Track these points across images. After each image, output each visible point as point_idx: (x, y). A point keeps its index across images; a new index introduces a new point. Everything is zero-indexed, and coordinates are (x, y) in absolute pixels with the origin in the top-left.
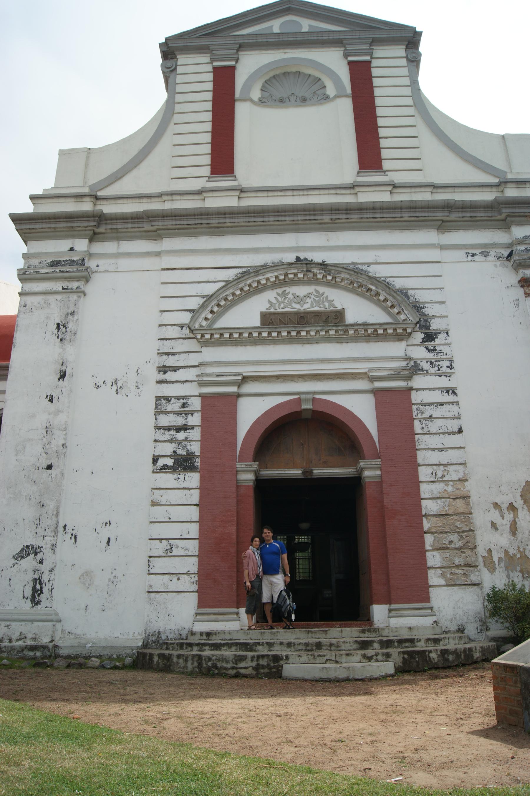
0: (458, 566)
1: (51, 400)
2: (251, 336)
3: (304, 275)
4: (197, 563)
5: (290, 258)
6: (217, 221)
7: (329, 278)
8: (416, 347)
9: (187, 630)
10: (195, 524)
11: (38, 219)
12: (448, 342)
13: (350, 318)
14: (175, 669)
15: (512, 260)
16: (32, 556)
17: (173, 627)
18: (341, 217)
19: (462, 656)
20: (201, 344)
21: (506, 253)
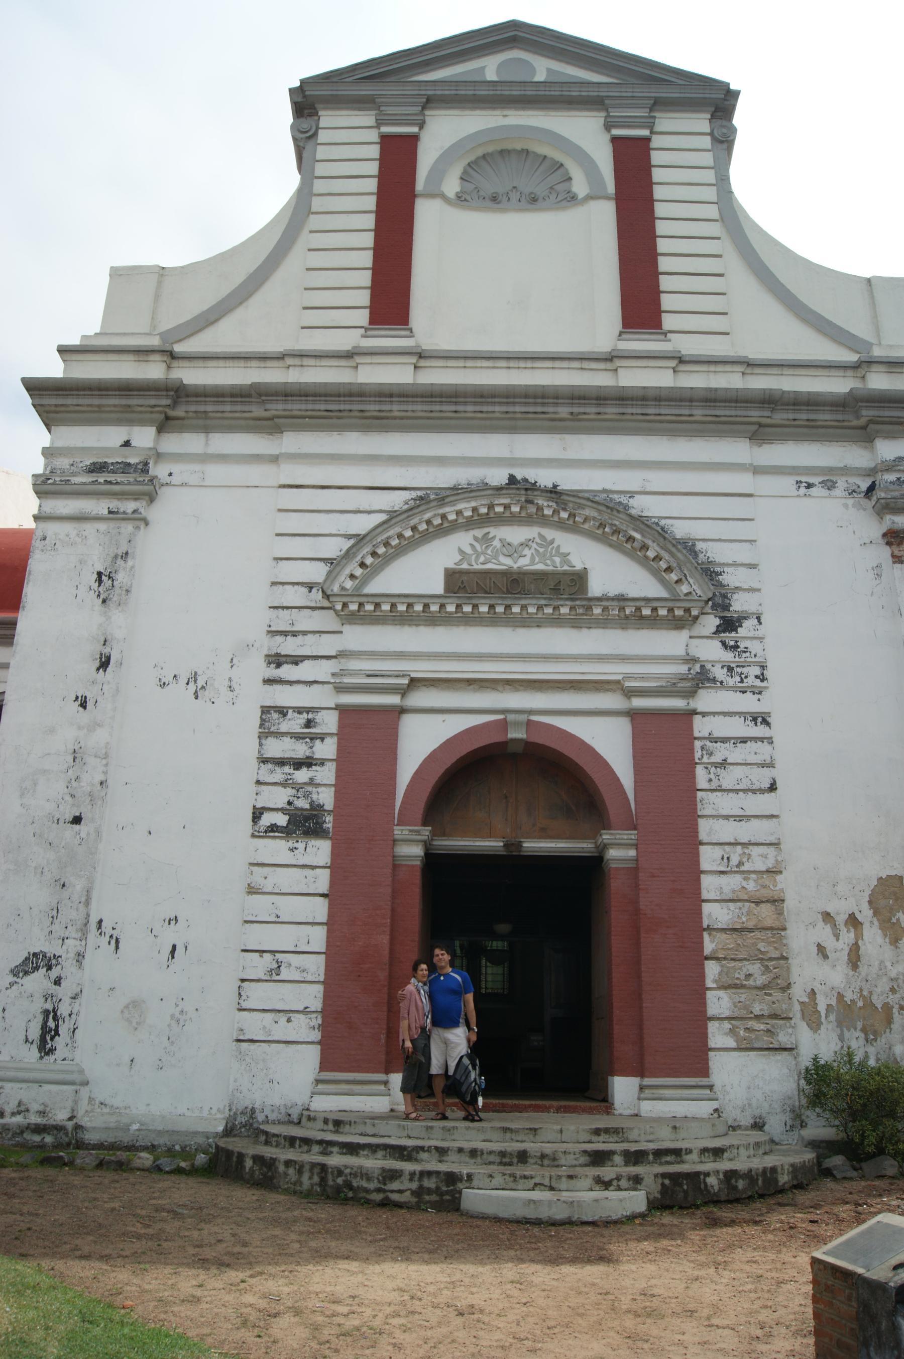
0: (758, 1017)
1: (83, 705)
2: (427, 610)
3: (521, 508)
4: (321, 995)
5: (498, 477)
6: (377, 407)
7: (564, 515)
8: (705, 640)
9: (301, 1108)
10: (320, 927)
11: (71, 389)
12: (759, 634)
13: (596, 587)
14: (281, 1183)
15: (874, 498)
16: (43, 971)
17: (277, 1102)
18: (588, 410)
19: (760, 1182)
20: (341, 619)
21: (864, 485)
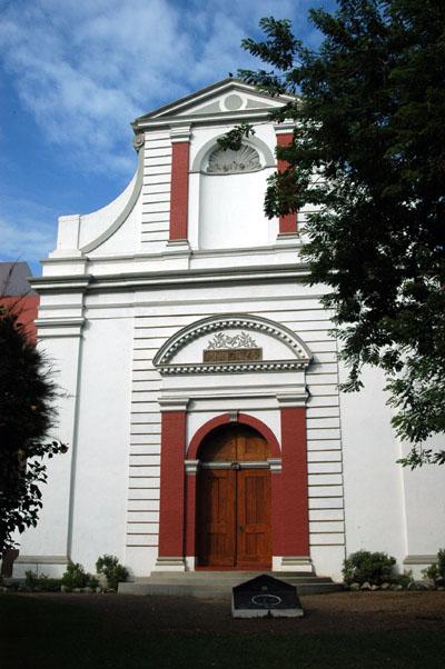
13: (266, 357)
